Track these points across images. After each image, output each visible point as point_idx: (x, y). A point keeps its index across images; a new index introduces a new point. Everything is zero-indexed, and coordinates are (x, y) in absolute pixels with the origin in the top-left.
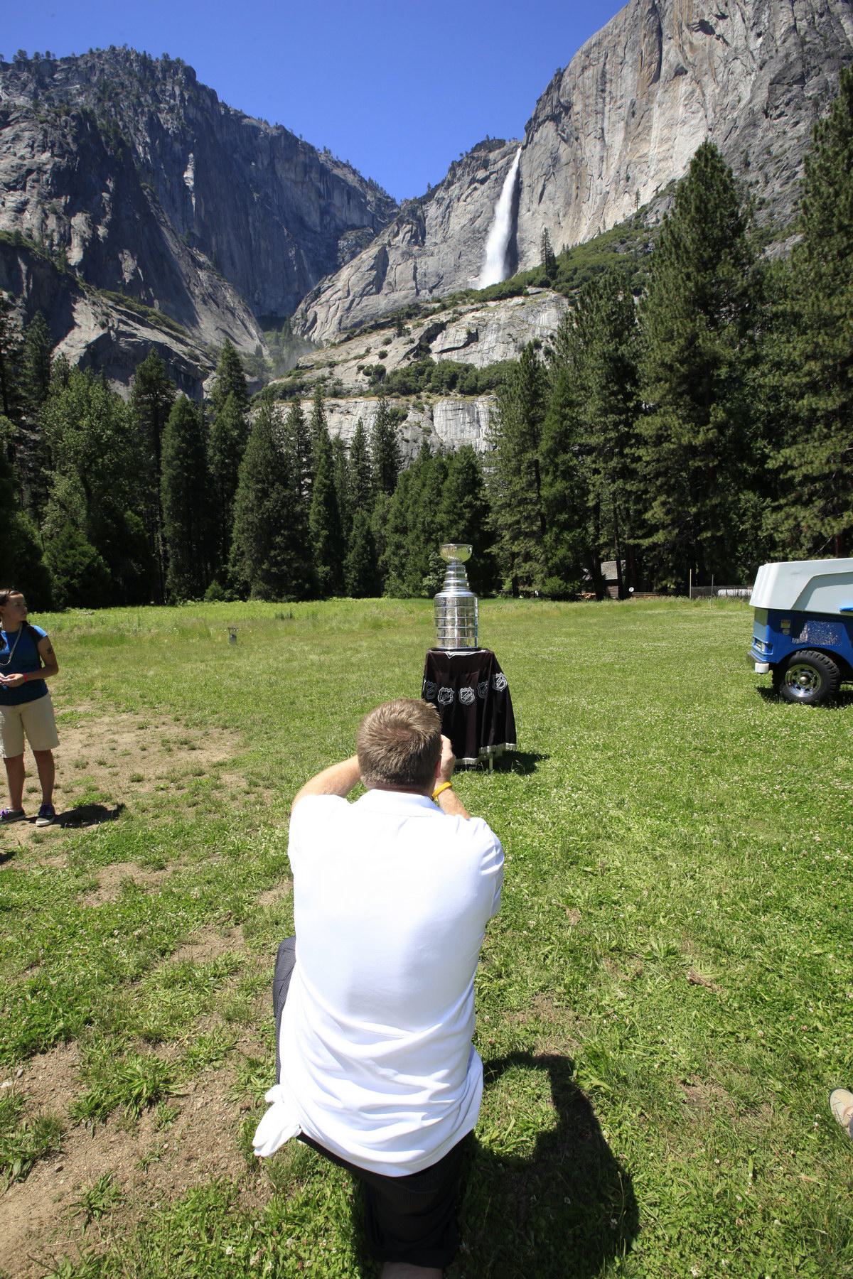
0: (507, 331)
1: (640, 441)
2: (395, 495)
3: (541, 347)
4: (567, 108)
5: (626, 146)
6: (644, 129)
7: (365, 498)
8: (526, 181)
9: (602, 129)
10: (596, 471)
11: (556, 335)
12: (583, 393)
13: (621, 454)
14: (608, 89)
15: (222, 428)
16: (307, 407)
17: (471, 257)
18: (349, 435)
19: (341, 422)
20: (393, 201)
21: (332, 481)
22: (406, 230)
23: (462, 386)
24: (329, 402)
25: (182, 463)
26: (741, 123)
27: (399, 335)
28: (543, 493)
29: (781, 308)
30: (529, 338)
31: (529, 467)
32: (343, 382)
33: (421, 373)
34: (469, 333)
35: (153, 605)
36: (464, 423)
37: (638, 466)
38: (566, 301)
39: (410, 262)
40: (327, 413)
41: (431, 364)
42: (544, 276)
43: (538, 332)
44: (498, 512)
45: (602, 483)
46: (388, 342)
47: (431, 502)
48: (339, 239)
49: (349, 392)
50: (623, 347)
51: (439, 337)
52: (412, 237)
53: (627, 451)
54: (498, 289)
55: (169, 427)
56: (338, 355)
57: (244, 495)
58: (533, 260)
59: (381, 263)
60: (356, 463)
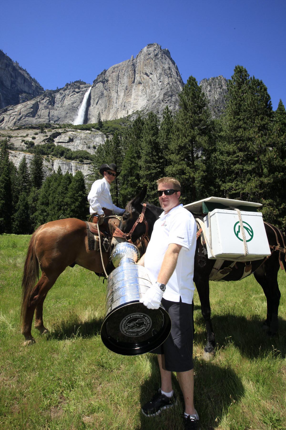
4: (107, 81)
5: (124, 97)
6: (130, 94)
8: (92, 97)
14: (120, 79)
17: (71, 115)
20: (43, 88)
22: (47, 99)
23: (66, 156)
26: (156, 101)
27: (42, 133)
33: (50, 148)
36: (66, 169)
38: (105, 136)
41: (54, 146)
43: (95, 143)
51: (58, 137)
52: (49, 102)
56: (13, 134)
58: (93, 121)
59: (36, 107)
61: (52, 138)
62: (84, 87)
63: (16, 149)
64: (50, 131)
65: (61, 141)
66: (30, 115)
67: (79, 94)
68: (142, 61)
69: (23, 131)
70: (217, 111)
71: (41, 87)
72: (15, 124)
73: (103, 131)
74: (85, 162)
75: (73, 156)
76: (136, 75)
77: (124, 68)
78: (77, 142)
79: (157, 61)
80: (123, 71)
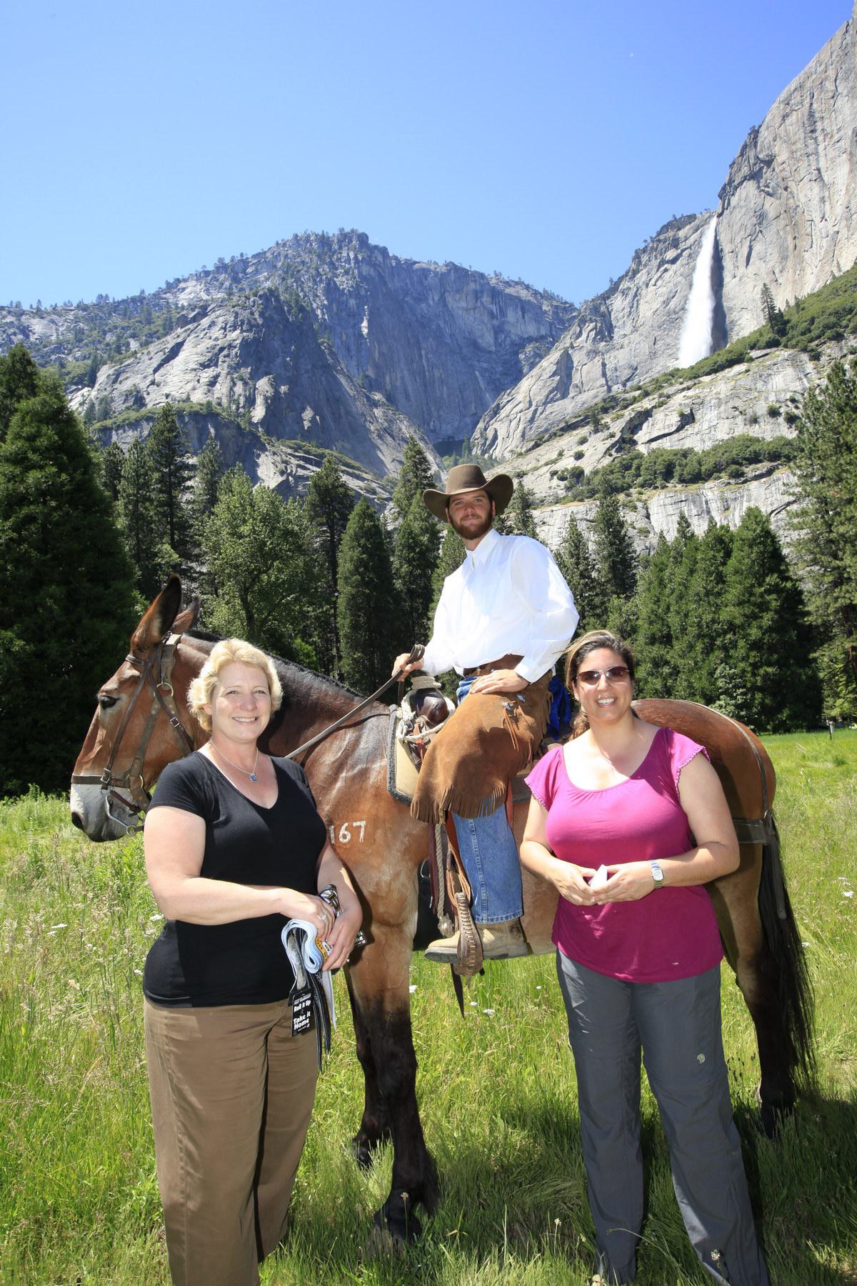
3: (779, 414)
4: (769, 162)
8: (726, 247)
9: (819, 170)
11: (798, 397)
14: (819, 126)
17: (668, 340)
20: (572, 305)
27: (596, 431)
32: (535, 491)
33: (628, 467)
39: (598, 360)
41: (639, 456)
42: (770, 335)
48: (517, 353)
49: (542, 501)
51: (645, 425)
54: (711, 362)
56: (525, 464)
58: (748, 323)
59: (565, 367)
62: (691, 231)
64: (618, 417)
65: (655, 434)
66: (555, 395)
67: (679, 262)
69: (547, 448)
71: (566, 303)
72: (523, 436)
73: (794, 342)
74: (750, 475)
75: (703, 469)
78: (708, 417)
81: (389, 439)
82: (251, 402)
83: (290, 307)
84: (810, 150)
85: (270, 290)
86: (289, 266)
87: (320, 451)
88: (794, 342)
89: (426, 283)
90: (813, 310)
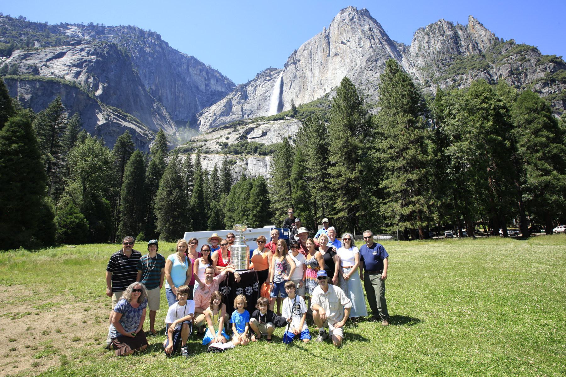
0: (278, 132)
1: (330, 176)
2: (229, 195)
4: (299, 61)
7: (216, 197)
8: (285, 82)
10: (314, 187)
12: (307, 157)
13: (323, 181)
15: (154, 164)
16: (193, 157)
17: (264, 105)
18: (211, 169)
19: (208, 164)
20: (234, 84)
21: (202, 188)
24: (203, 155)
25: (133, 178)
26: (358, 71)
27: (235, 131)
28: (293, 196)
29: (377, 131)
30: (287, 135)
31: (287, 185)
34: (263, 132)
35: (109, 243)
37: (331, 186)
39: (240, 105)
40: (202, 160)
41: (247, 143)
44: (273, 203)
45: (316, 192)
46: (230, 133)
47: (245, 199)
50: (322, 141)
53: (325, 180)
55: (129, 162)
56: (208, 137)
57: (161, 193)
58: (287, 108)
60: (213, 181)
61: (245, 135)
63: (212, 152)
64: (243, 128)
68: (336, 30)
70: (440, 65)
72: (211, 125)
76: (331, 47)
77: (317, 43)
78: (270, 134)
79: (353, 25)
80: (316, 46)
81: (157, 116)
82: (96, 88)
83: (122, 54)
84: (310, 62)
85: (114, 44)
86: (124, 37)
87: (126, 114)
88: (298, 117)
89: (182, 61)
90: (304, 109)
